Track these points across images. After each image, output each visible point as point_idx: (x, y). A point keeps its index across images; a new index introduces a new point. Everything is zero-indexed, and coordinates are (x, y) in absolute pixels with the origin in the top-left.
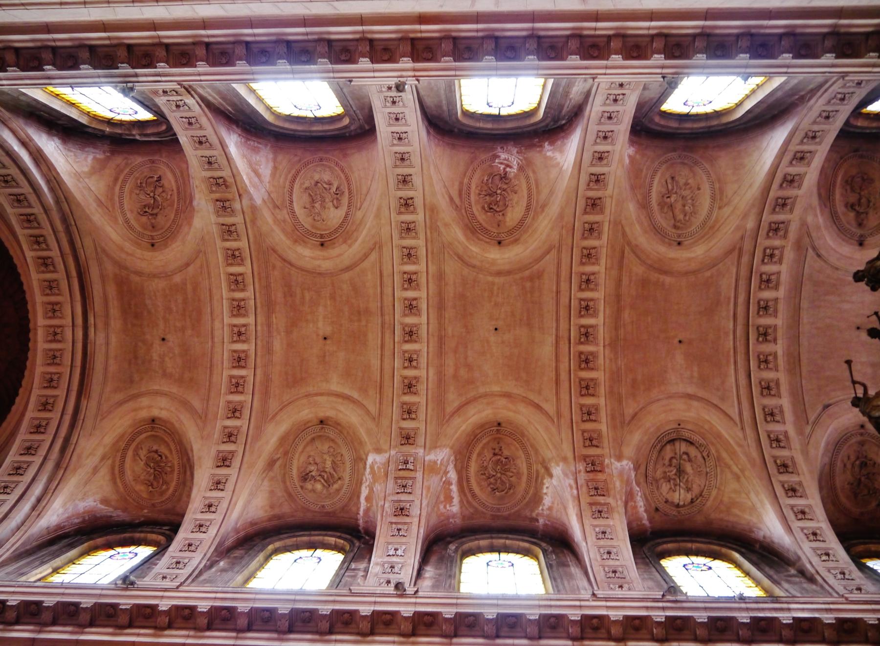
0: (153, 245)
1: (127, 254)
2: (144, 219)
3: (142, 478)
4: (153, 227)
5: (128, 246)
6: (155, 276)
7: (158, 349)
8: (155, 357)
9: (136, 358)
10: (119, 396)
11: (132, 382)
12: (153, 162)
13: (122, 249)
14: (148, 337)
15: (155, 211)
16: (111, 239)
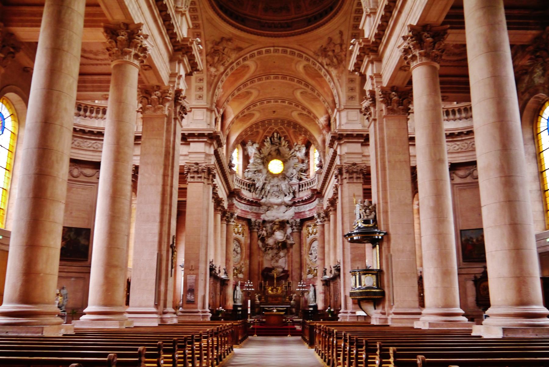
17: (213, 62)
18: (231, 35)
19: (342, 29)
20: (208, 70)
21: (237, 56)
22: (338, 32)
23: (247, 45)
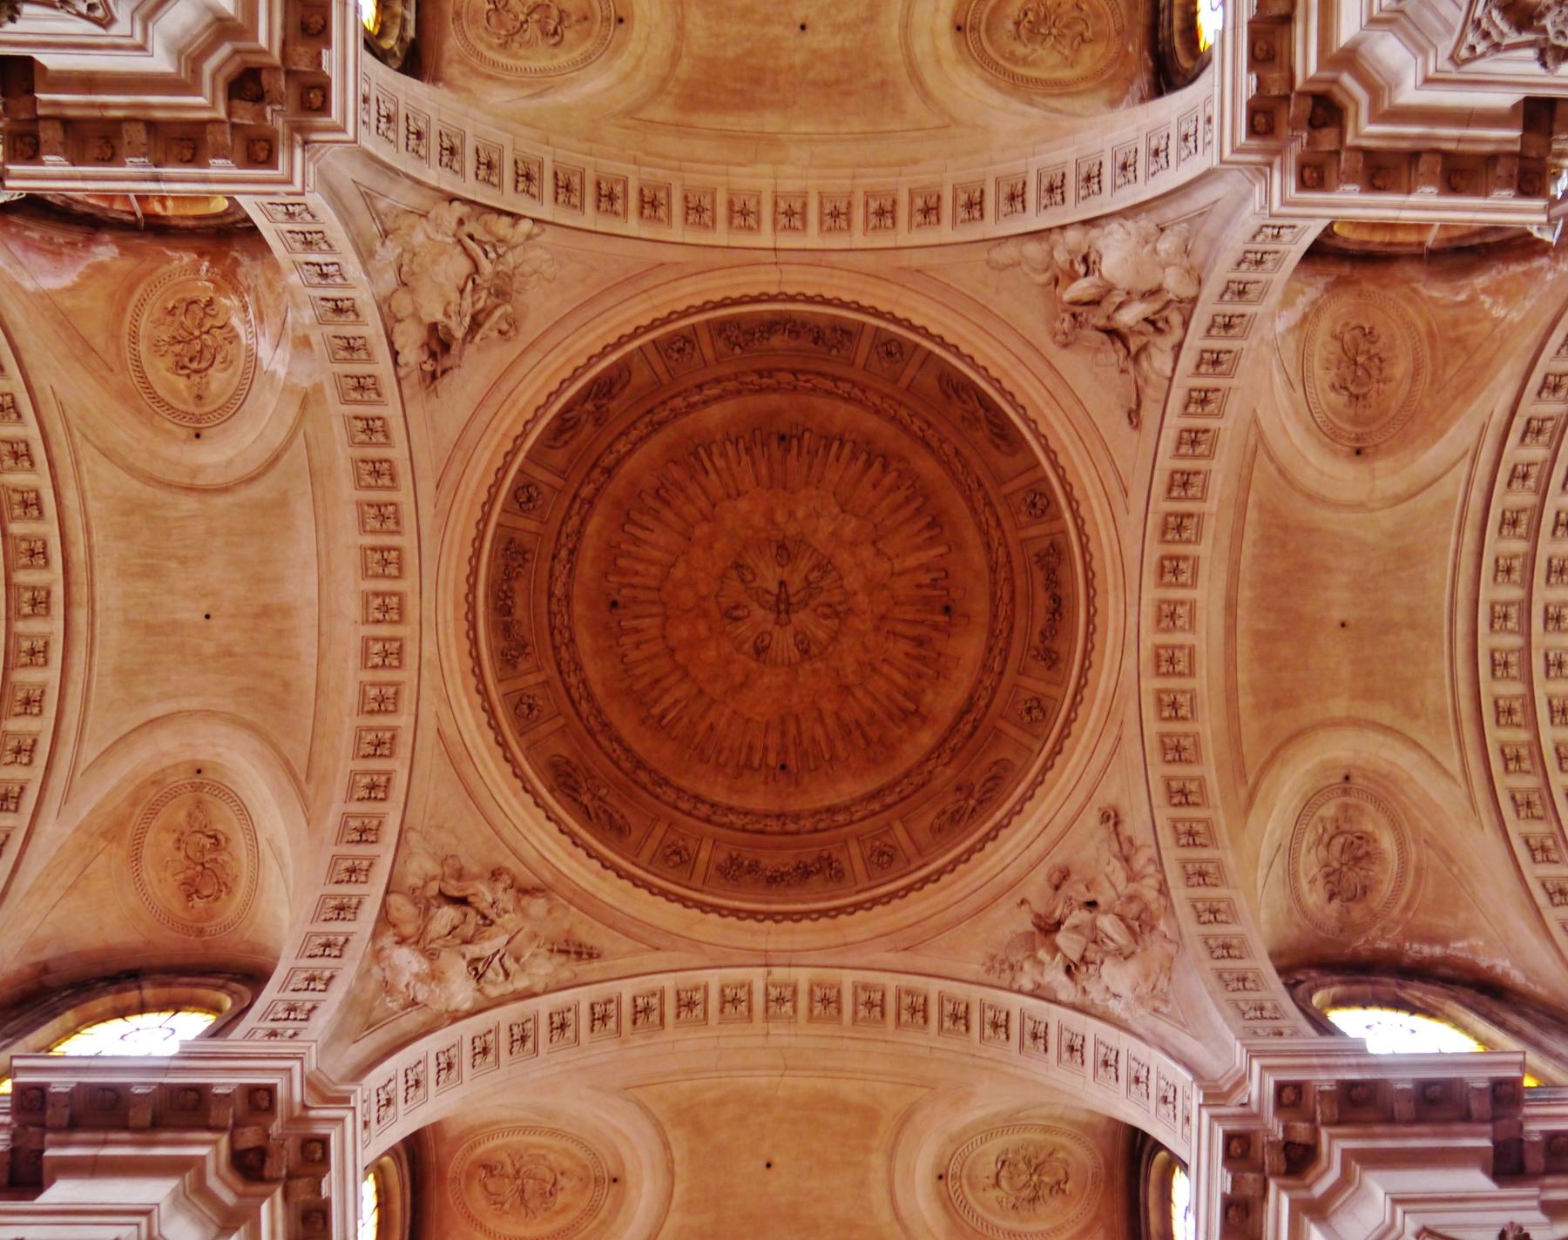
0: (621, 21)
1: (636, 68)
2: (569, 35)
3: (1067, 52)
4: (586, 19)
5: (623, 63)
6: (680, 29)
7: (823, 39)
8: (836, 42)
9: (837, 82)
10: (912, 101)
11: (883, 84)
12: (458, 15)
13: (626, 77)
14: (798, 59)
15: (555, 13)
16: (608, 89)
17: (422, 933)
18: (547, 876)
19: (1110, 794)
20: (377, 955)
21: (565, 974)
22: (1091, 818)
23: (625, 944)
